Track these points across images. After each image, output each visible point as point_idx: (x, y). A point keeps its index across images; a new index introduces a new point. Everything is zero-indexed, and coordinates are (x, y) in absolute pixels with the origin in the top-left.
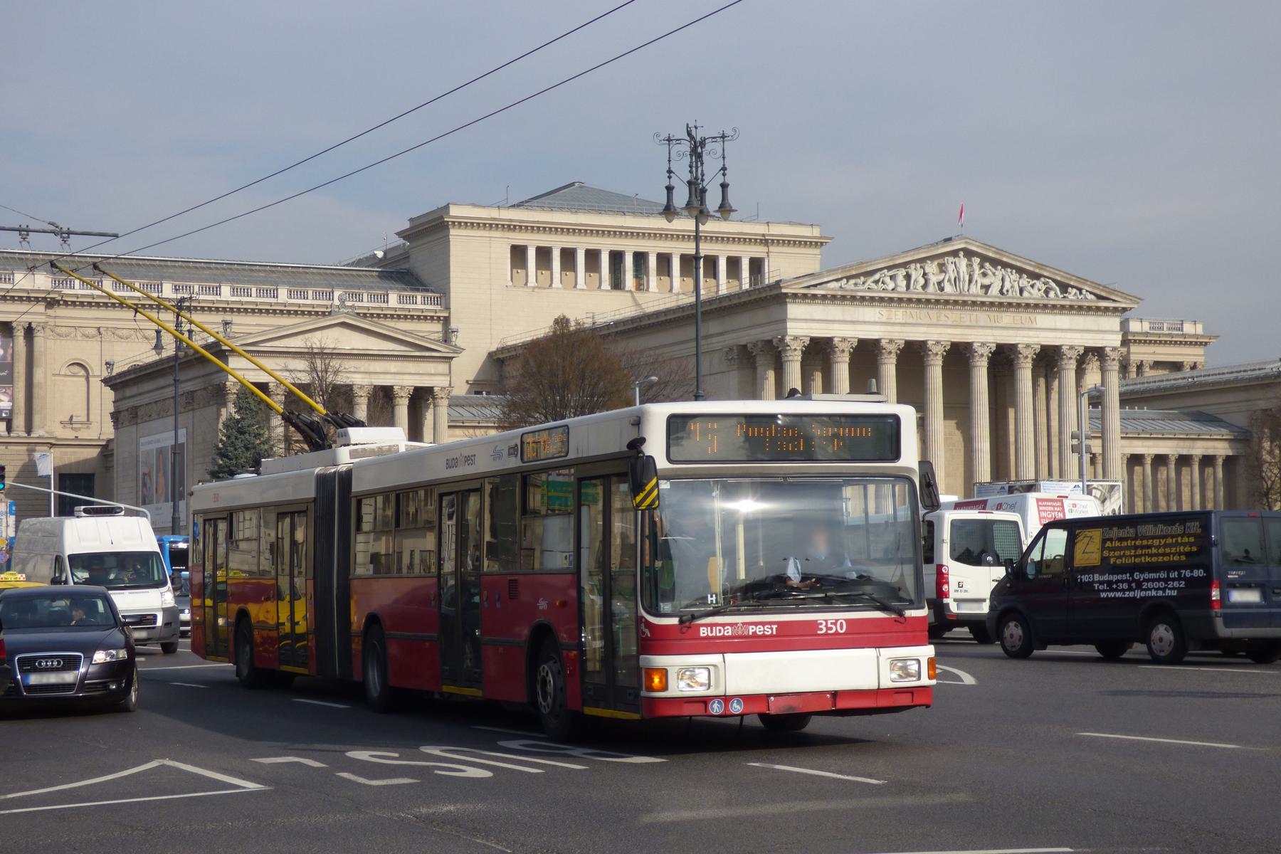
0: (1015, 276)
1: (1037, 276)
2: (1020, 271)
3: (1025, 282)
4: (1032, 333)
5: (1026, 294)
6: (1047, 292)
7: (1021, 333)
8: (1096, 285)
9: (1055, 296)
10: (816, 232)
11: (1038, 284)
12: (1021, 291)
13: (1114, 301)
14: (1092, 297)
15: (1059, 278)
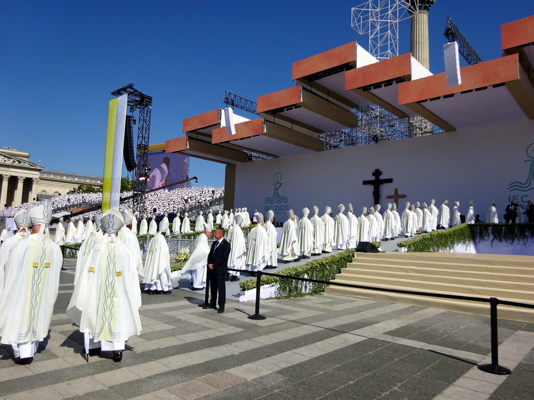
0: (3, 157)
1: (11, 158)
2: (5, 156)
3: (6, 159)
4: (8, 172)
5: (6, 162)
6: (14, 162)
7: (5, 172)
8: (30, 163)
9: (17, 164)
10: (27, 154)
11: (11, 160)
12: (5, 161)
13: (36, 167)
14: (27, 165)
15: (18, 159)
